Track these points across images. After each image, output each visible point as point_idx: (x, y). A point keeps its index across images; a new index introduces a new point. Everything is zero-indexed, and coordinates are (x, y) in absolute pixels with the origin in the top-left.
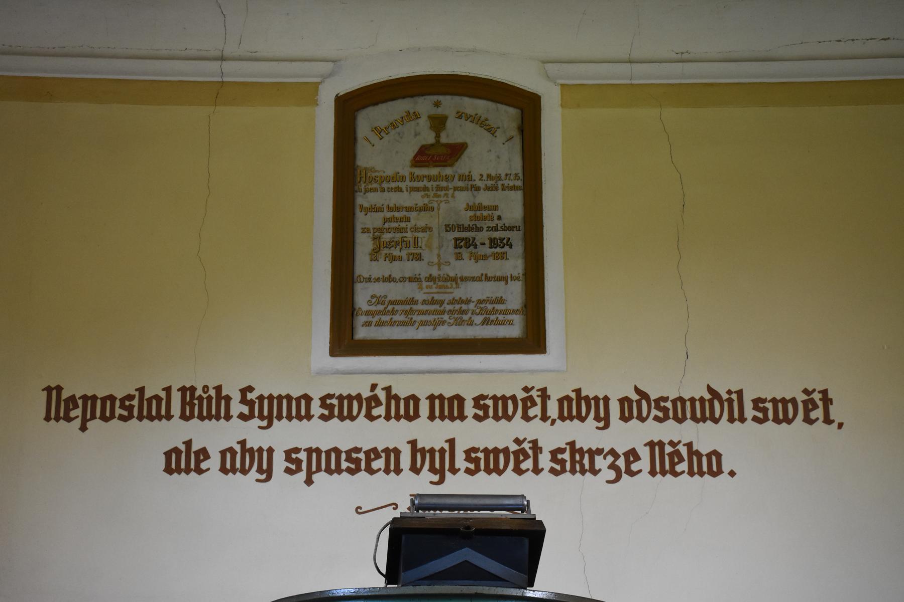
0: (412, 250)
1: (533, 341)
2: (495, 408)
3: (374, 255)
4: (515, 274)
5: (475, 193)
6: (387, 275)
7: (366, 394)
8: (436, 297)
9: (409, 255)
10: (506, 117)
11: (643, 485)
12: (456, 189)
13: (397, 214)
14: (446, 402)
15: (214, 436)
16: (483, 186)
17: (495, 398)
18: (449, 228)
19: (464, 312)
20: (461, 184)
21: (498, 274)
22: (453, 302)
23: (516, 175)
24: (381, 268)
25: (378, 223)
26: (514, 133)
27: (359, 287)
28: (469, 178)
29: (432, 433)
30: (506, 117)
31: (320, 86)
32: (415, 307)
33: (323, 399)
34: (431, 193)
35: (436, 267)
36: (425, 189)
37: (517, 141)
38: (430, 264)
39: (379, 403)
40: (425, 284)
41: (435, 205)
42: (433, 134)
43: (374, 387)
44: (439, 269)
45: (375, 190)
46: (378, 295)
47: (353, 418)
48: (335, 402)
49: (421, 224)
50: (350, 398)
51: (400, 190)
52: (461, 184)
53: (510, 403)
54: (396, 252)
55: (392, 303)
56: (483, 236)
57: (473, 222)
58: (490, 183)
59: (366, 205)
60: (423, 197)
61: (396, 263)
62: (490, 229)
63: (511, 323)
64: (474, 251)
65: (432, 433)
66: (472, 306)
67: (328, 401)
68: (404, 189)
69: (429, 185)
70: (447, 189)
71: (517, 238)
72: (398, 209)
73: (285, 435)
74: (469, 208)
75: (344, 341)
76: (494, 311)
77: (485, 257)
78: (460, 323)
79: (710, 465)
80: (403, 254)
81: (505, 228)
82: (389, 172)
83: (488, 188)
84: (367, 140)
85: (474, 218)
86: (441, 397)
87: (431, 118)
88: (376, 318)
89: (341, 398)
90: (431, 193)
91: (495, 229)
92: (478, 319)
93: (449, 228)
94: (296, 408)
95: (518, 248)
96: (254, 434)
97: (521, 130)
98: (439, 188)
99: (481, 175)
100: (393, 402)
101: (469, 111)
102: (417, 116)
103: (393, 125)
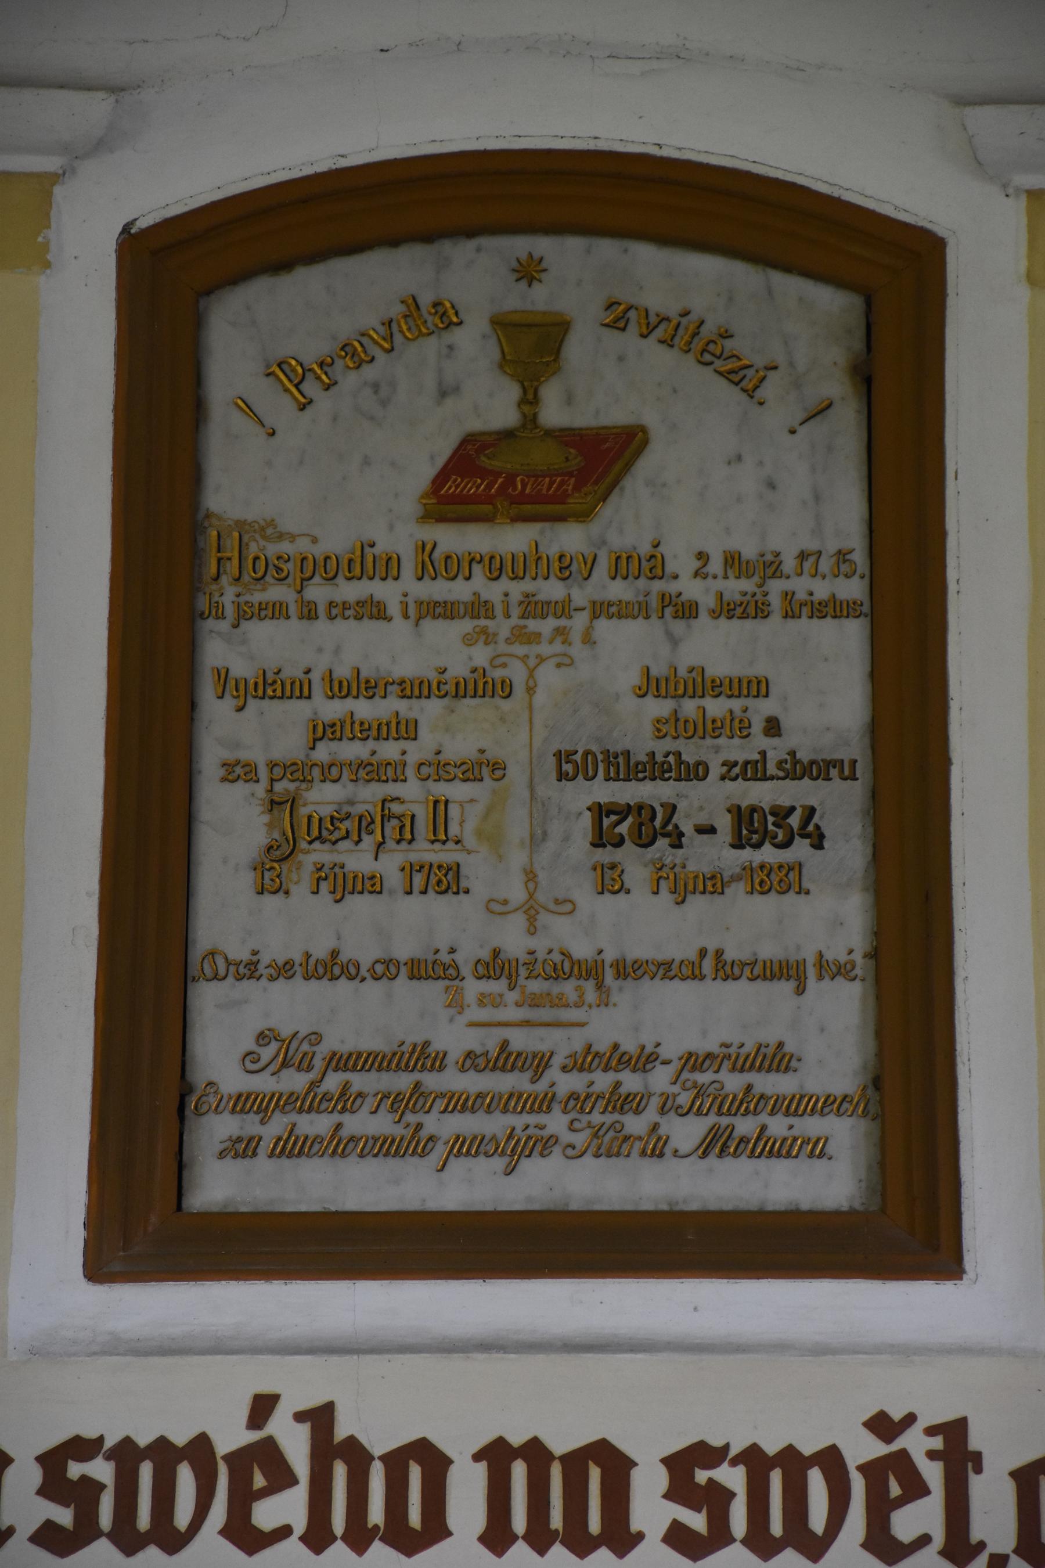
0: (425, 852)
3: (272, 870)
4: (836, 953)
5: (678, 627)
6: (320, 952)
7: (231, 1436)
8: (520, 1040)
9: (410, 870)
10: (805, 321)
12: (600, 609)
13: (364, 709)
14: (556, 1472)
16: (707, 601)
17: (754, 1460)
18: (570, 766)
19: (624, 1103)
20: (619, 590)
21: (769, 951)
22: (584, 1061)
23: (842, 556)
25: (290, 744)
26: (836, 386)
27: (208, 999)
28: (654, 565)
30: (805, 321)
31: (57, 190)
32: (431, 1081)
33: (53, 1461)
34: (503, 628)
35: (519, 921)
36: (479, 608)
37: (847, 423)
38: (496, 908)
39: (282, 1477)
40: (473, 988)
41: (517, 673)
42: (513, 392)
43: (262, 1407)
44: (532, 930)
45: (276, 611)
46: (286, 1032)
47: (173, 1541)
48: (101, 1470)
49: (461, 747)
50: (164, 1453)
51: (373, 610)
52: (619, 590)
53: (816, 1480)
54: (358, 859)
55: (339, 1062)
56: (706, 800)
57: (668, 744)
58: (736, 587)
59: (241, 669)
60: (468, 640)
61: (360, 904)
62: (733, 771)
63: (817, 1150)
64: (673, 857)
66: (660, 1079)
67: (75, 1470)
68: (394, 609)
69: (493, 592)
70: (564, 609)
71: (842, 809)
72: (370, 688)
74: (652, 685)
75: (145, 1220)
76: (749, 1102)
77: (714, 884)
78: (611, 1146)
80: (390, 866)
81: (796, 769)
82: (336, 540)
83: (726, 610)
84: (248, 409)
85: (673, 725)
86: (535, 1452)
87: (504, 325)
88: (277, 1125)
89: (126, 1455)
90: (503, 628)
91: (754, 770)
92: (686, 1132)
93: (570, 766)
95: (848, 847)
97: (864, 376)
98: (532, 607)
99: (702, 556)
100: (340, 1472)
101: (657, 299)
102: (446, 317)
103: (353, 353)
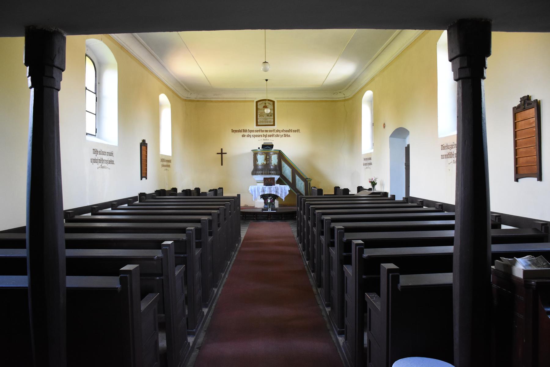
1: (274, 125)
2: (271, 131)
11: (283, 138)
15: (246, 134)
29: (265, 133)
30: (272, 103)
65: (265, 133)
73: (252, 134)
75: (257, 125)
79: (289, 136)
94: (253, 131)
96: (249, 134)
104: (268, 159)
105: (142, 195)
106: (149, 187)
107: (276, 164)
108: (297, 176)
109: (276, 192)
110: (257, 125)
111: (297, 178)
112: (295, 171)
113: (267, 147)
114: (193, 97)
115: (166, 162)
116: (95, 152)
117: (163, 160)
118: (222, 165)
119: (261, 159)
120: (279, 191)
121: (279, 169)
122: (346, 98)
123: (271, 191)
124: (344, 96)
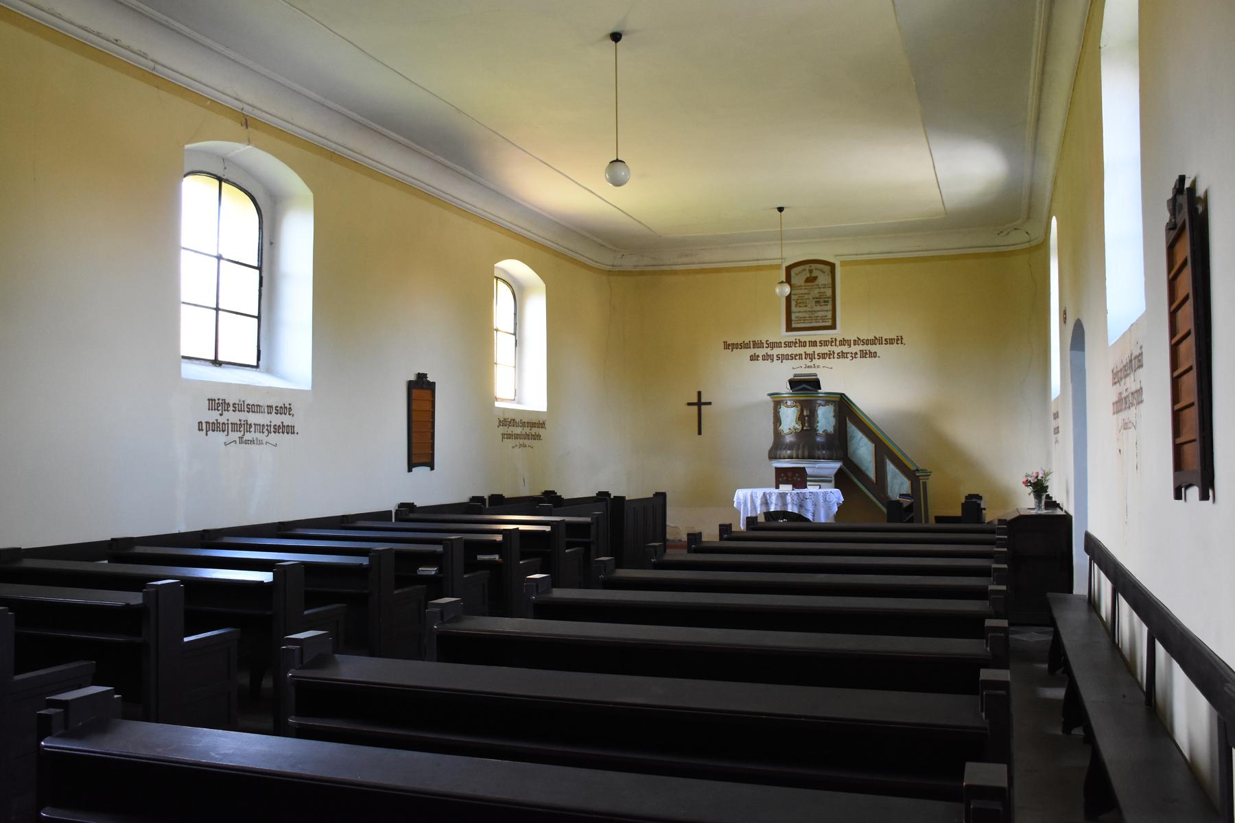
1: (833, 327)
2: (824, 343)
10: (827, 269)
11: (858, 360)
15: (760, 352)
24: (798, 309)
29: (809, 350)
30: (827, 269)
65: (809, 350)
73: (776, 351)
75: (789, 328)
79: (874, 355)
94: (778, 345)
104: (807, 417)
105: (406, 509)
106: (431, 489)
107: (831, 429)
108: (888, 462)
109: (801, 506)
110: (789, 328)
111: (890, 467)
112: (883, 451)
113: (805, 386)
114: (629, 263)
115: (523, 429)
116: (217, 404)
117: (504, 422)
118: (700, 433)
119: (789, 417)
120: (810, 506)
121: (837, 445)
122: (1034, 243)
123: (785, 504)
124: (1026, 238)
